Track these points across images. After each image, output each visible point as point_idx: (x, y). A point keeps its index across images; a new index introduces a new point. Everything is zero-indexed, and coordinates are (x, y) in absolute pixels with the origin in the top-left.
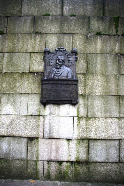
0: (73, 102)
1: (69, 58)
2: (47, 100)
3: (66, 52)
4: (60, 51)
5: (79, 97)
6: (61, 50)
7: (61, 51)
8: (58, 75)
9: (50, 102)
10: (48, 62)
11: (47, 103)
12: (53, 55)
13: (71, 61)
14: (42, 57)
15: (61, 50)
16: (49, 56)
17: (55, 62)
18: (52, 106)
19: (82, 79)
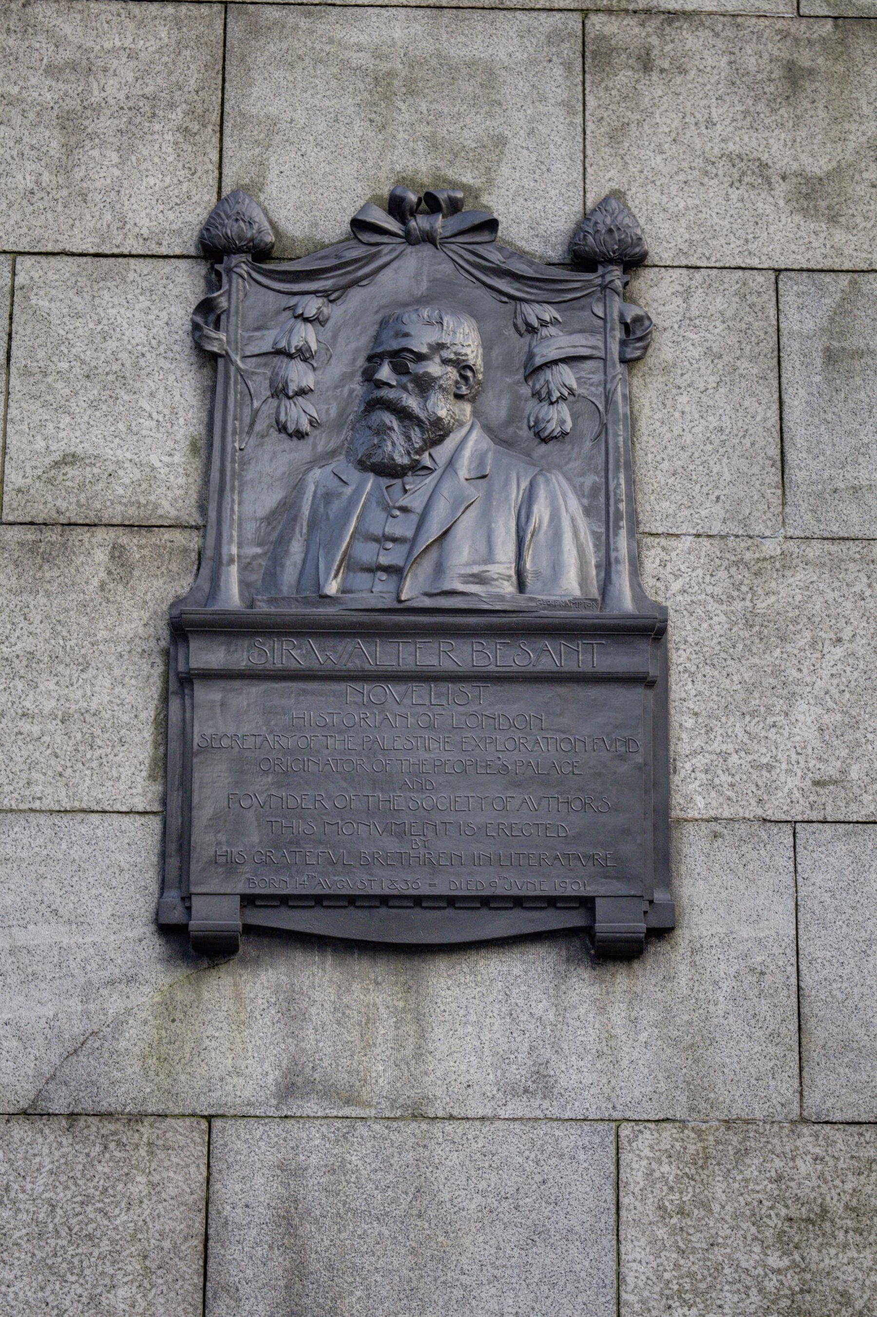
0: (610, 921)
1: (532, 330)
2: (248, 901)
3: (496, 257)
4: (410, 239)
5: (693, 851)
6: (420, 223)
7: (429, 238)
8: (392, 556)
10: (260, 386)
12: (325, 294)
13: (567, 375)
14: (179, 313)
15: (420, 223)
16: (273, 301)
17: (357, 387)
18: (320, 981)
19: (712, 606)
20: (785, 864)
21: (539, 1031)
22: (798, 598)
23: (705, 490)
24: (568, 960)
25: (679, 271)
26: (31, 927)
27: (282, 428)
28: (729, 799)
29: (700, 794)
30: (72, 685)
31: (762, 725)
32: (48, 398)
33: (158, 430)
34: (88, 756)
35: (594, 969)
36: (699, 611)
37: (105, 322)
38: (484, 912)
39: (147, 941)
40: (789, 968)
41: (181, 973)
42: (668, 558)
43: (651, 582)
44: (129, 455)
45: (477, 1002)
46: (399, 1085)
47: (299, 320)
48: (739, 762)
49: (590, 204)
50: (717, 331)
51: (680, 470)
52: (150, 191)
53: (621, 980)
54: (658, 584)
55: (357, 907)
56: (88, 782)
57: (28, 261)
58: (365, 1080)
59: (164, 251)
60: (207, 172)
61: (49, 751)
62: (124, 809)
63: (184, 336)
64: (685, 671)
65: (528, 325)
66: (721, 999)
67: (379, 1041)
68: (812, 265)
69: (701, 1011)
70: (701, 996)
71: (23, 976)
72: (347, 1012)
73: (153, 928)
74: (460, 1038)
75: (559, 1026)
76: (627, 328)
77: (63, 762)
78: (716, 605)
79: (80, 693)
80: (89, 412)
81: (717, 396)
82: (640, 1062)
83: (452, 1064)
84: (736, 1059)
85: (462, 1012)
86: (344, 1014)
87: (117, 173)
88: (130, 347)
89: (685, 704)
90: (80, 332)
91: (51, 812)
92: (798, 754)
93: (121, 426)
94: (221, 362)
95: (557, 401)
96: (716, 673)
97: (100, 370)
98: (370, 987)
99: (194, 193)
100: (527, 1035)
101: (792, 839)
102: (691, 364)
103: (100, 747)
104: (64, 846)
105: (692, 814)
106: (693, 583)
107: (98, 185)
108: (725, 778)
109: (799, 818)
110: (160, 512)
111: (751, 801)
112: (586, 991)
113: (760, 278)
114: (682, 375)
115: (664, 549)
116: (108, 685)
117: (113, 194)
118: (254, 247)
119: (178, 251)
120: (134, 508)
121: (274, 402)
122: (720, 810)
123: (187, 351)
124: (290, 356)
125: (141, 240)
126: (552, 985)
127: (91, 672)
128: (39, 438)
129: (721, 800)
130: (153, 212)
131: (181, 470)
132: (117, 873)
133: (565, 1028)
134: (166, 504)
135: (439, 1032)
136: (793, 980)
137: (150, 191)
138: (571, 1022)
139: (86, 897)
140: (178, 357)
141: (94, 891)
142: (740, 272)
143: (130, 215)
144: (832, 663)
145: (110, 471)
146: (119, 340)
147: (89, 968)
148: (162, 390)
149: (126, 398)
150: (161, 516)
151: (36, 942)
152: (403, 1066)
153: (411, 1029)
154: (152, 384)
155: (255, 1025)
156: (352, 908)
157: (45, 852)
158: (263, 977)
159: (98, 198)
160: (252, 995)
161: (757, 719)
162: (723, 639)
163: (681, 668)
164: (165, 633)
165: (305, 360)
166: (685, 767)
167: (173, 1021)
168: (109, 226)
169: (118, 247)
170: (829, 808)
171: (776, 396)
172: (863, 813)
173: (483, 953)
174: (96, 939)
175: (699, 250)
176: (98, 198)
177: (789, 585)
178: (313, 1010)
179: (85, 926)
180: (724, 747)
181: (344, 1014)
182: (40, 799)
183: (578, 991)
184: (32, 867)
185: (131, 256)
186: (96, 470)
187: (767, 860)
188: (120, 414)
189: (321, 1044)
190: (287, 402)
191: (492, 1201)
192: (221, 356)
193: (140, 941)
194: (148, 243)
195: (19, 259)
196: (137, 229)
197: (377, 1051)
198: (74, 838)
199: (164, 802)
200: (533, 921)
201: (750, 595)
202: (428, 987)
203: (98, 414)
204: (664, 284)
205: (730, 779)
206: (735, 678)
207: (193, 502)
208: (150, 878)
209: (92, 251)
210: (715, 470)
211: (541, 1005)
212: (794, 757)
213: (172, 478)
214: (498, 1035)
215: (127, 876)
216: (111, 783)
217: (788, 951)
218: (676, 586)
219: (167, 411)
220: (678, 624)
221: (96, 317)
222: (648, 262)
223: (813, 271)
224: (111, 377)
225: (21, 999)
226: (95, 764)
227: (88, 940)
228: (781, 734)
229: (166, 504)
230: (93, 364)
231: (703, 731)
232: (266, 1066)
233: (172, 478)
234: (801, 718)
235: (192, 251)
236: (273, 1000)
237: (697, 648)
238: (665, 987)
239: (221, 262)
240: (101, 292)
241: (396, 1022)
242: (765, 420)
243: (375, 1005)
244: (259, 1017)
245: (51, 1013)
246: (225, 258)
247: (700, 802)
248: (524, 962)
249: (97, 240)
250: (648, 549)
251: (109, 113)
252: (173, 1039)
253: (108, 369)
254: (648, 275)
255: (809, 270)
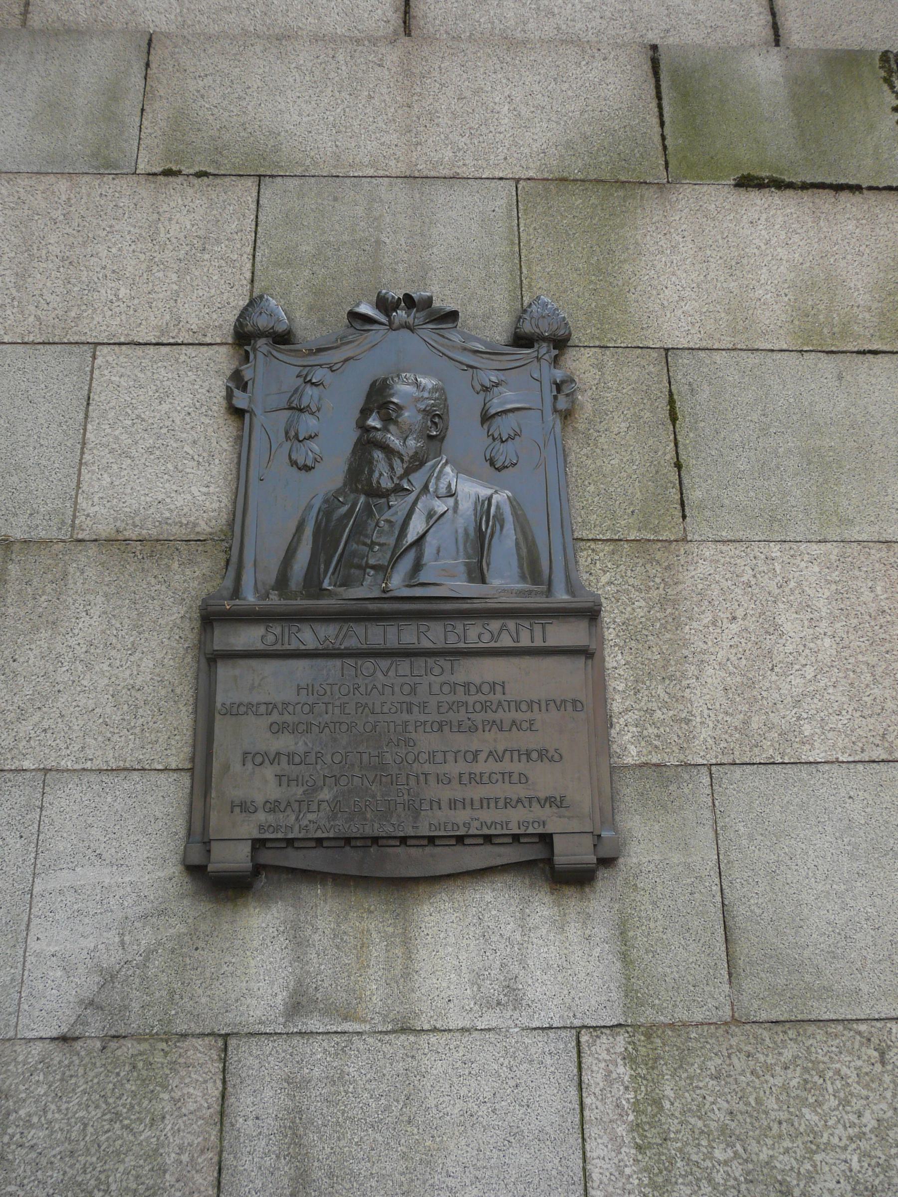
9: (295, 859)
11: (258, 869)
19: (634, 594)
20: (705, 800)
21: (508, 950)
22: (700, 586)
23: (624, 506)
24: (531, 885)
25: (593, 350)
26: (78, 869)
27: (294, 463)
28: (656, 747)
29: (632, 743)
30: (122, 666)
31: (678, 687)
32: (114, 446)
33: (198, 469)
34: (132, 724)
35: (553, 894)
36: (624, 598)
37: (161, 390)
38: (459, 848)
39: (176, 879)
40: (714, 888)
41: (205, 907)
42: (597, 557)
43: (585, 576)
44: (175, 488)
45: (454, 925)
46: (389, 1001)
47: (309, 385)
48: (662, 717)
49: (525, 304)
50: (624, 391)
51: (603, 491)
52: (199, 299)
53: (573, 901)
54: (592, 578)
55: (352, 847)
56: (131, 745)
57: (105, 350)
58: (361, 998)
59: (208, 340)
60: (242, 286)
61: (101, 720)
62: (160, 767)
63: (221, 400)
64: (616, 645)
65: (483, 386)
66: (660, 917)
67: (372, 963)
68: (691, 345)
69: (644, 928)
70: (643, 914)
71: (70, 912)
72: (345, 938)
73: (180, 867)
74: (441, 959)
75: (525, 945)
76: (559, 387)
77: (112, 730)
78: (637, 593)
79: (128, 672)
80: (145, 456)
81: (628, 437)
82: (594, 974)
83: (435, 981)
84: (675, 969)
85: (442, 935)
86: (342, 939)
87: (175, 287)
88: (179, 408)
89: (617, 671)
90: (142, 398)
91: (100, 771)
92: (709, 709)
93: (169, 466)
94: (247, 416)
95: (506, 440)
96: (640, 646)
97: (155, 426)
98: (365, 915)
99: (232, 299)
100: (498, 954)
101: (709, 779)
102: (607, 415)
103: (142, 716)
104: (109, 800)
105: (629, 760)
106: (618, 577)
107: (161, 296)
108: (652, 730)
109: (714, 761)
110: (198, 529)
111: (674, 748)
112: (546, 913)
113: (654, 354)
114: (601, 422)
115: (593, 550)
116: (151, 666)
117: (172, 303)
118: (274, 332)
119: (218, 340)
120: (177, 527)
121: (289, 443)
122: (650, 757)
123: (223, 410)
124: (301, 410)
125: (191, 333)
126: (518, 909)
127: (138, 655)
128: (105, 476)
129: (650, 748)
130: (201, 314)
131: (215, 498)
132: (153, 821)
133: (530, 946)
134: (203, 525)
135: (423, 953)
136: (718, 898)
137: (199, 299)
138: (535, 940)
139: (126, 843)
140: (216, 415)
141: (132, 838)
142: (640, 350)
143: (184, 315)
144: (730, 637)
145: (160, 499)
146: (171, 403)
147: (126, 904)
148: (202, 439)
149: (175, 445)
150: (198, 533)
151: (82, 882)
152: (394, 985)
153: (398, 951)
154: (195, 435)
155: (263, 955)
156: (348, 848)
157: (93, 805)
158: (274, 911)
159: (160, 305)
160: (264, 925)
161: (674, 682)
162: (643, 620)
163: (612, 643)
164: (197, 624)
165: (313, 414)
166: (619, 722)
167: (197, 949)
168: (167, 324)
169: (173, 338)
170: (737, 753)
171: (672, 437)
172: (764, 756)
173: (459, 882)
174: (132, 878)
175: (609, 336)
176: (160, 305)
177: (693, 577)
178: (316, 937)
179: (124, 867)
180: (650, 705)
181: (342, 939)
182: (91, 760)
183: (539, 914)
184: (81, 818)
185: (182, 344)
186: (148, 499)
187: (690, 796)
188: (169, 457)
189: (322, 967)
190: (299, 444)
191: (472, 1106)
192: (248, 412)
193: (171, 879)
194: (196, 335)
195: (99, 348)
196: (189, 326)
197: (370, 972)
198: (118, 793)
199: (192, 760)
200: (500, 856)
201: (662, 585)
202: (413, 914)
203: (152, 457)
204: (584, 359)
205: (656, 731)
206: (654, 650)
207: (224, 522)
208: (180, 826)
209: (154, 341)
210: (630, 492)
211: (509, 926)
212: (706, 712)
213: (208, 503)
214: (473, 955)
215: (161, 824)
216: (151, 746)
217: (712, 873)
218: (604, 579)
219: (205, 454)
220: (608, 608)
221: (155, 388)
222: (569, 343)
223: (692, 349)
224: (164, 431)
225: (67, 933)
226: (137, 730)
227: (127, 879)
228: (695, 694)
229: (203, 525)
230: (150, 421)
231: (632, 693)
232: (276, 989)
233: (208, 503)
234: (709, 680)
235: (230, 340)
236: (281, 929)
237: (624, 627)
238: (612, 908)
239: (249, 344)
240: (159, 370)
241: (386, 946)
242: (665, 454)
243: (368, 930)
244: (269, 944)
245: (92, 945)
246: (252, 342)
247: (633, 750)
248: (494, 890)
249: (158, 334)
250: (582, 550)
251: (171, 248)
252: (196, 965)
253: (161, 425)
254: (571, 353)
255: (689, 349)
